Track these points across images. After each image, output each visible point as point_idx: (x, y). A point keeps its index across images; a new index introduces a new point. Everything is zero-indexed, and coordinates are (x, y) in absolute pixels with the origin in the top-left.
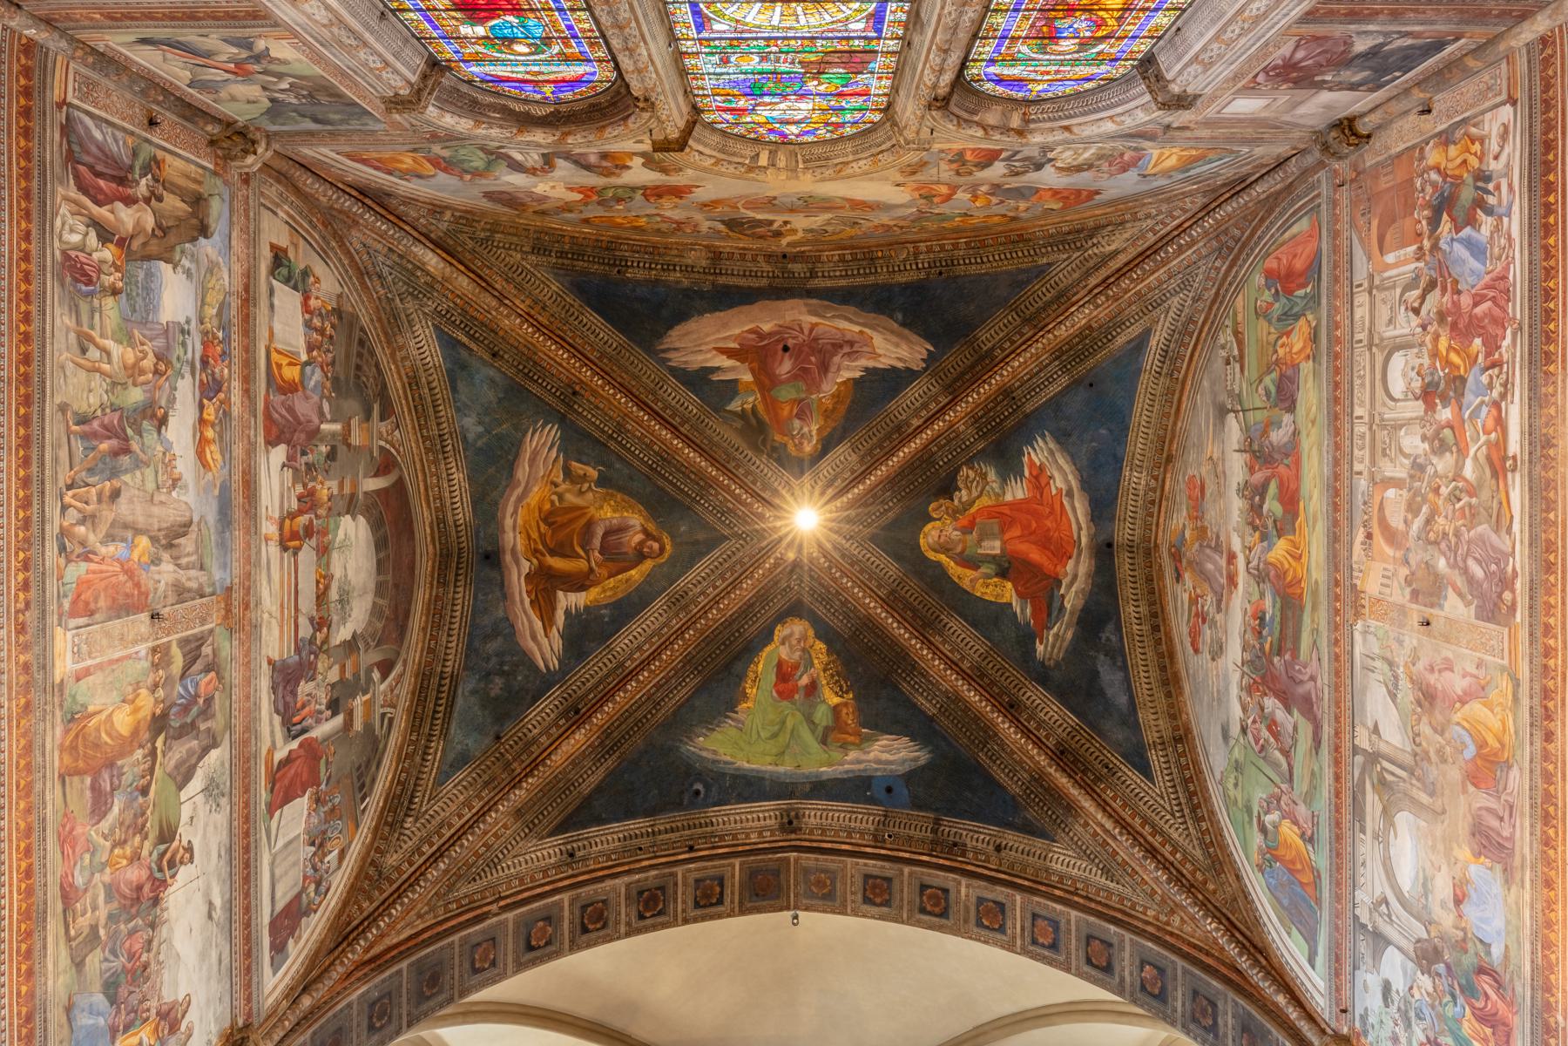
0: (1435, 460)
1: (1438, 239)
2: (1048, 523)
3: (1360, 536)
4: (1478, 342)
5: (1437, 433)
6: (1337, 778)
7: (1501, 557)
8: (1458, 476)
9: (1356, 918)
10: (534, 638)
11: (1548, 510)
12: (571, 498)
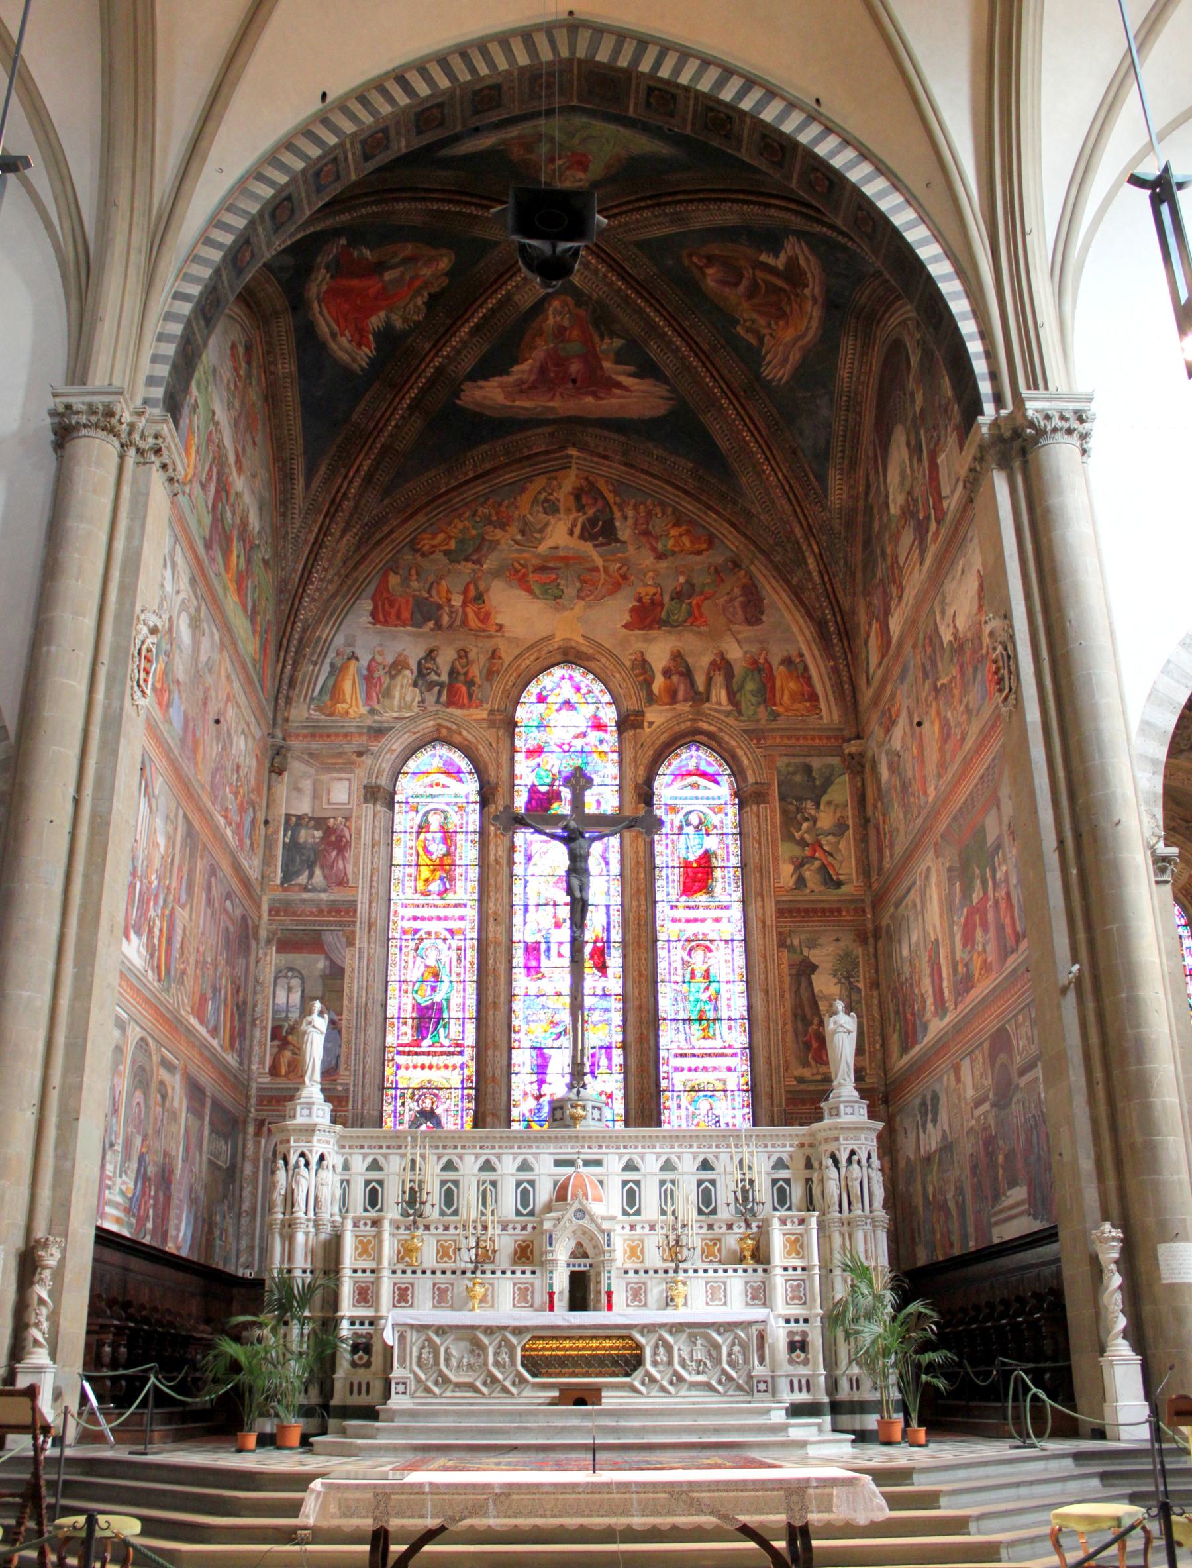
2: (347, 307)
10: (807, 259)
12: (762, 322)
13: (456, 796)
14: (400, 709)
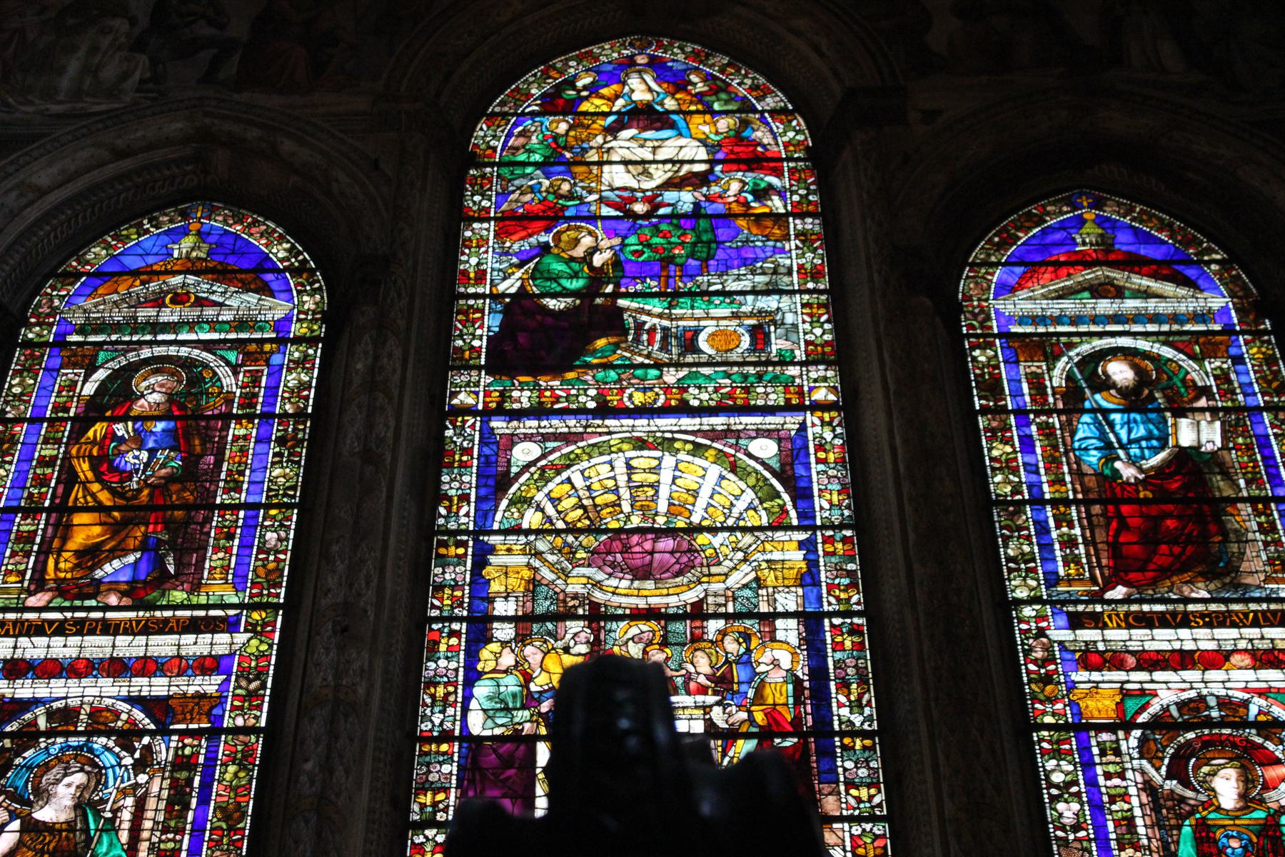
13: (240, 324)
14: (77, 94)
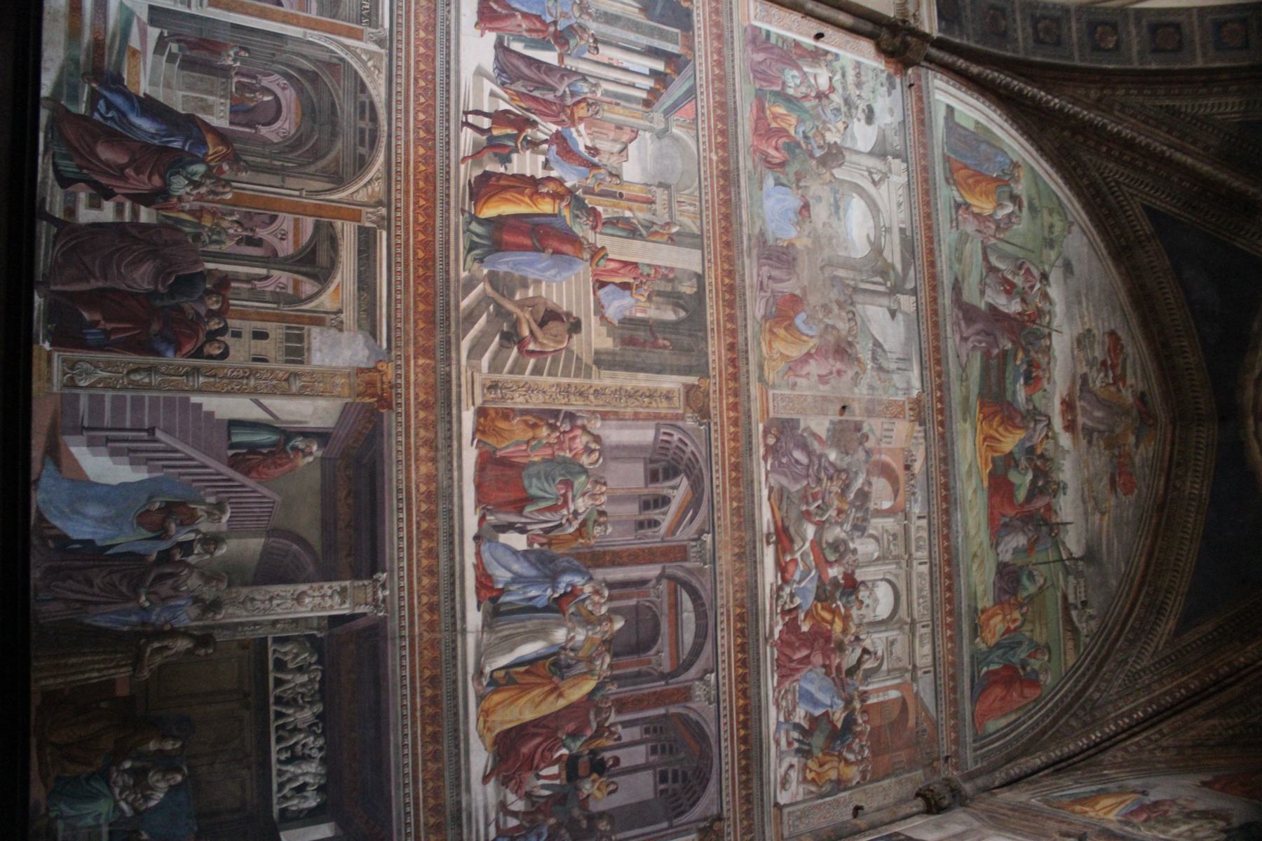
0: (843, 535)
1: (846, 708)
3: (918, 467)
4: (805, 628)
5: (842, 556)
6: (932, 264)
7: (778, 468)
8: (821, 526)
9: (906, 160)
11: (738, 508)
